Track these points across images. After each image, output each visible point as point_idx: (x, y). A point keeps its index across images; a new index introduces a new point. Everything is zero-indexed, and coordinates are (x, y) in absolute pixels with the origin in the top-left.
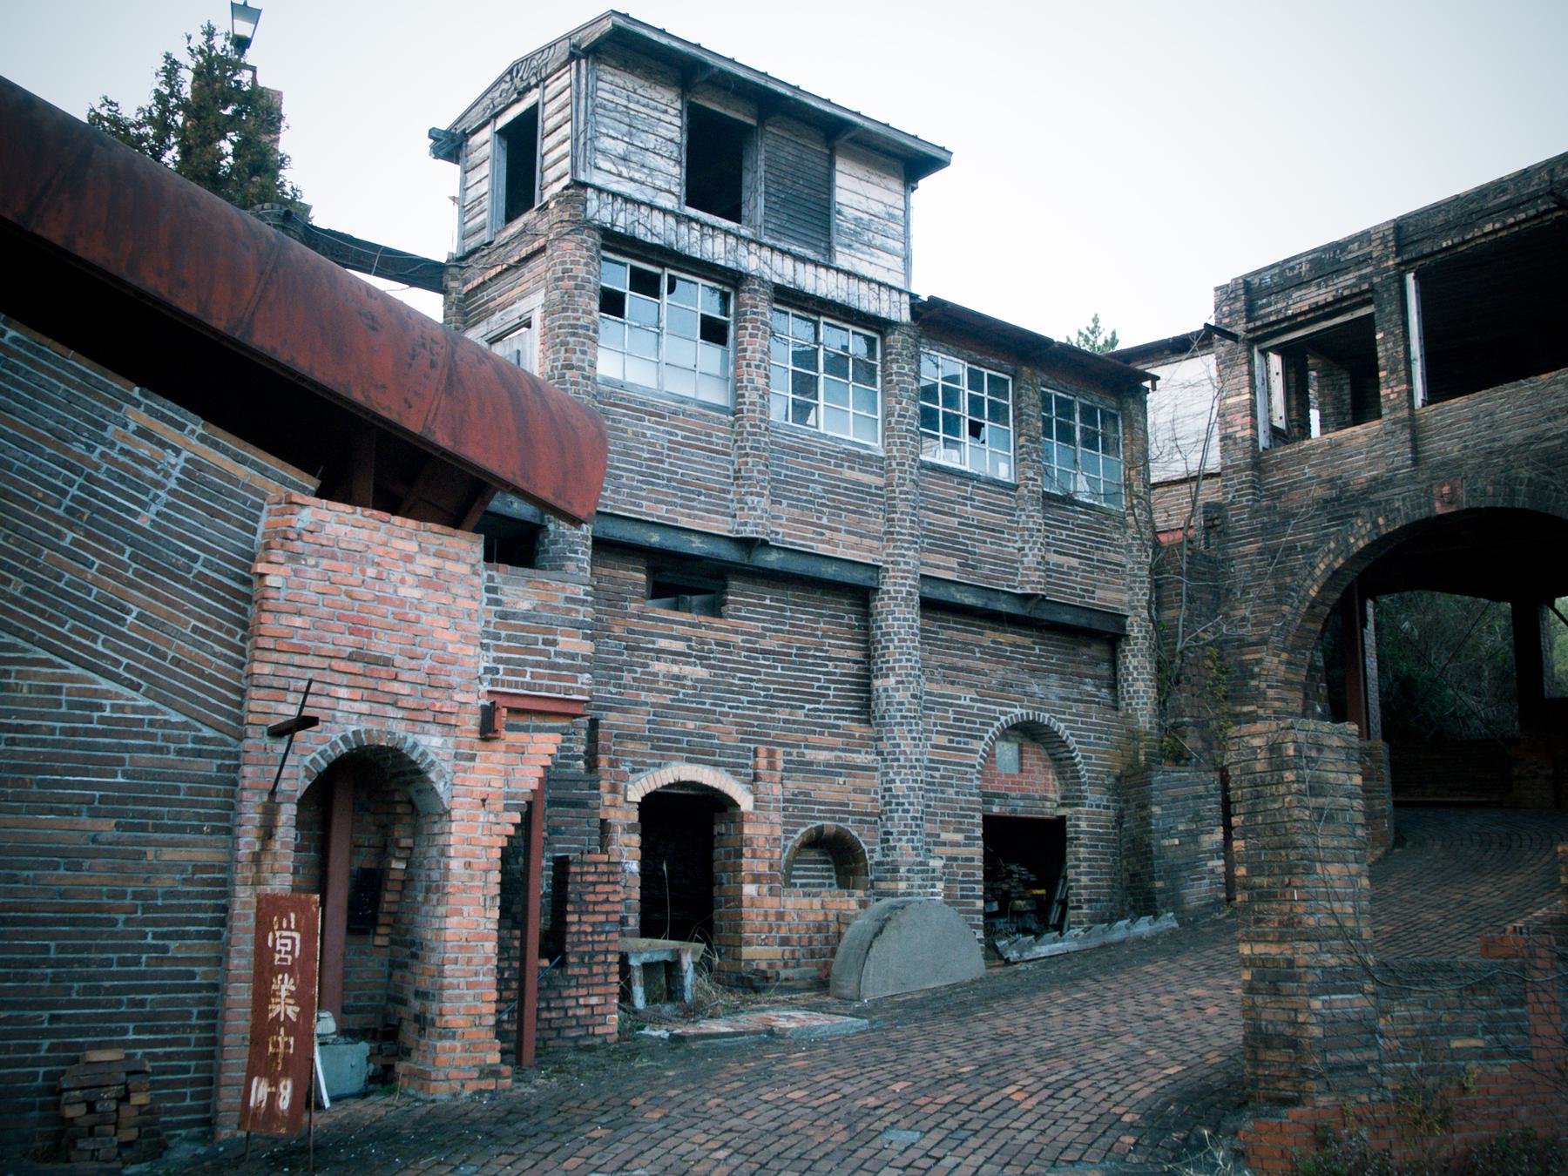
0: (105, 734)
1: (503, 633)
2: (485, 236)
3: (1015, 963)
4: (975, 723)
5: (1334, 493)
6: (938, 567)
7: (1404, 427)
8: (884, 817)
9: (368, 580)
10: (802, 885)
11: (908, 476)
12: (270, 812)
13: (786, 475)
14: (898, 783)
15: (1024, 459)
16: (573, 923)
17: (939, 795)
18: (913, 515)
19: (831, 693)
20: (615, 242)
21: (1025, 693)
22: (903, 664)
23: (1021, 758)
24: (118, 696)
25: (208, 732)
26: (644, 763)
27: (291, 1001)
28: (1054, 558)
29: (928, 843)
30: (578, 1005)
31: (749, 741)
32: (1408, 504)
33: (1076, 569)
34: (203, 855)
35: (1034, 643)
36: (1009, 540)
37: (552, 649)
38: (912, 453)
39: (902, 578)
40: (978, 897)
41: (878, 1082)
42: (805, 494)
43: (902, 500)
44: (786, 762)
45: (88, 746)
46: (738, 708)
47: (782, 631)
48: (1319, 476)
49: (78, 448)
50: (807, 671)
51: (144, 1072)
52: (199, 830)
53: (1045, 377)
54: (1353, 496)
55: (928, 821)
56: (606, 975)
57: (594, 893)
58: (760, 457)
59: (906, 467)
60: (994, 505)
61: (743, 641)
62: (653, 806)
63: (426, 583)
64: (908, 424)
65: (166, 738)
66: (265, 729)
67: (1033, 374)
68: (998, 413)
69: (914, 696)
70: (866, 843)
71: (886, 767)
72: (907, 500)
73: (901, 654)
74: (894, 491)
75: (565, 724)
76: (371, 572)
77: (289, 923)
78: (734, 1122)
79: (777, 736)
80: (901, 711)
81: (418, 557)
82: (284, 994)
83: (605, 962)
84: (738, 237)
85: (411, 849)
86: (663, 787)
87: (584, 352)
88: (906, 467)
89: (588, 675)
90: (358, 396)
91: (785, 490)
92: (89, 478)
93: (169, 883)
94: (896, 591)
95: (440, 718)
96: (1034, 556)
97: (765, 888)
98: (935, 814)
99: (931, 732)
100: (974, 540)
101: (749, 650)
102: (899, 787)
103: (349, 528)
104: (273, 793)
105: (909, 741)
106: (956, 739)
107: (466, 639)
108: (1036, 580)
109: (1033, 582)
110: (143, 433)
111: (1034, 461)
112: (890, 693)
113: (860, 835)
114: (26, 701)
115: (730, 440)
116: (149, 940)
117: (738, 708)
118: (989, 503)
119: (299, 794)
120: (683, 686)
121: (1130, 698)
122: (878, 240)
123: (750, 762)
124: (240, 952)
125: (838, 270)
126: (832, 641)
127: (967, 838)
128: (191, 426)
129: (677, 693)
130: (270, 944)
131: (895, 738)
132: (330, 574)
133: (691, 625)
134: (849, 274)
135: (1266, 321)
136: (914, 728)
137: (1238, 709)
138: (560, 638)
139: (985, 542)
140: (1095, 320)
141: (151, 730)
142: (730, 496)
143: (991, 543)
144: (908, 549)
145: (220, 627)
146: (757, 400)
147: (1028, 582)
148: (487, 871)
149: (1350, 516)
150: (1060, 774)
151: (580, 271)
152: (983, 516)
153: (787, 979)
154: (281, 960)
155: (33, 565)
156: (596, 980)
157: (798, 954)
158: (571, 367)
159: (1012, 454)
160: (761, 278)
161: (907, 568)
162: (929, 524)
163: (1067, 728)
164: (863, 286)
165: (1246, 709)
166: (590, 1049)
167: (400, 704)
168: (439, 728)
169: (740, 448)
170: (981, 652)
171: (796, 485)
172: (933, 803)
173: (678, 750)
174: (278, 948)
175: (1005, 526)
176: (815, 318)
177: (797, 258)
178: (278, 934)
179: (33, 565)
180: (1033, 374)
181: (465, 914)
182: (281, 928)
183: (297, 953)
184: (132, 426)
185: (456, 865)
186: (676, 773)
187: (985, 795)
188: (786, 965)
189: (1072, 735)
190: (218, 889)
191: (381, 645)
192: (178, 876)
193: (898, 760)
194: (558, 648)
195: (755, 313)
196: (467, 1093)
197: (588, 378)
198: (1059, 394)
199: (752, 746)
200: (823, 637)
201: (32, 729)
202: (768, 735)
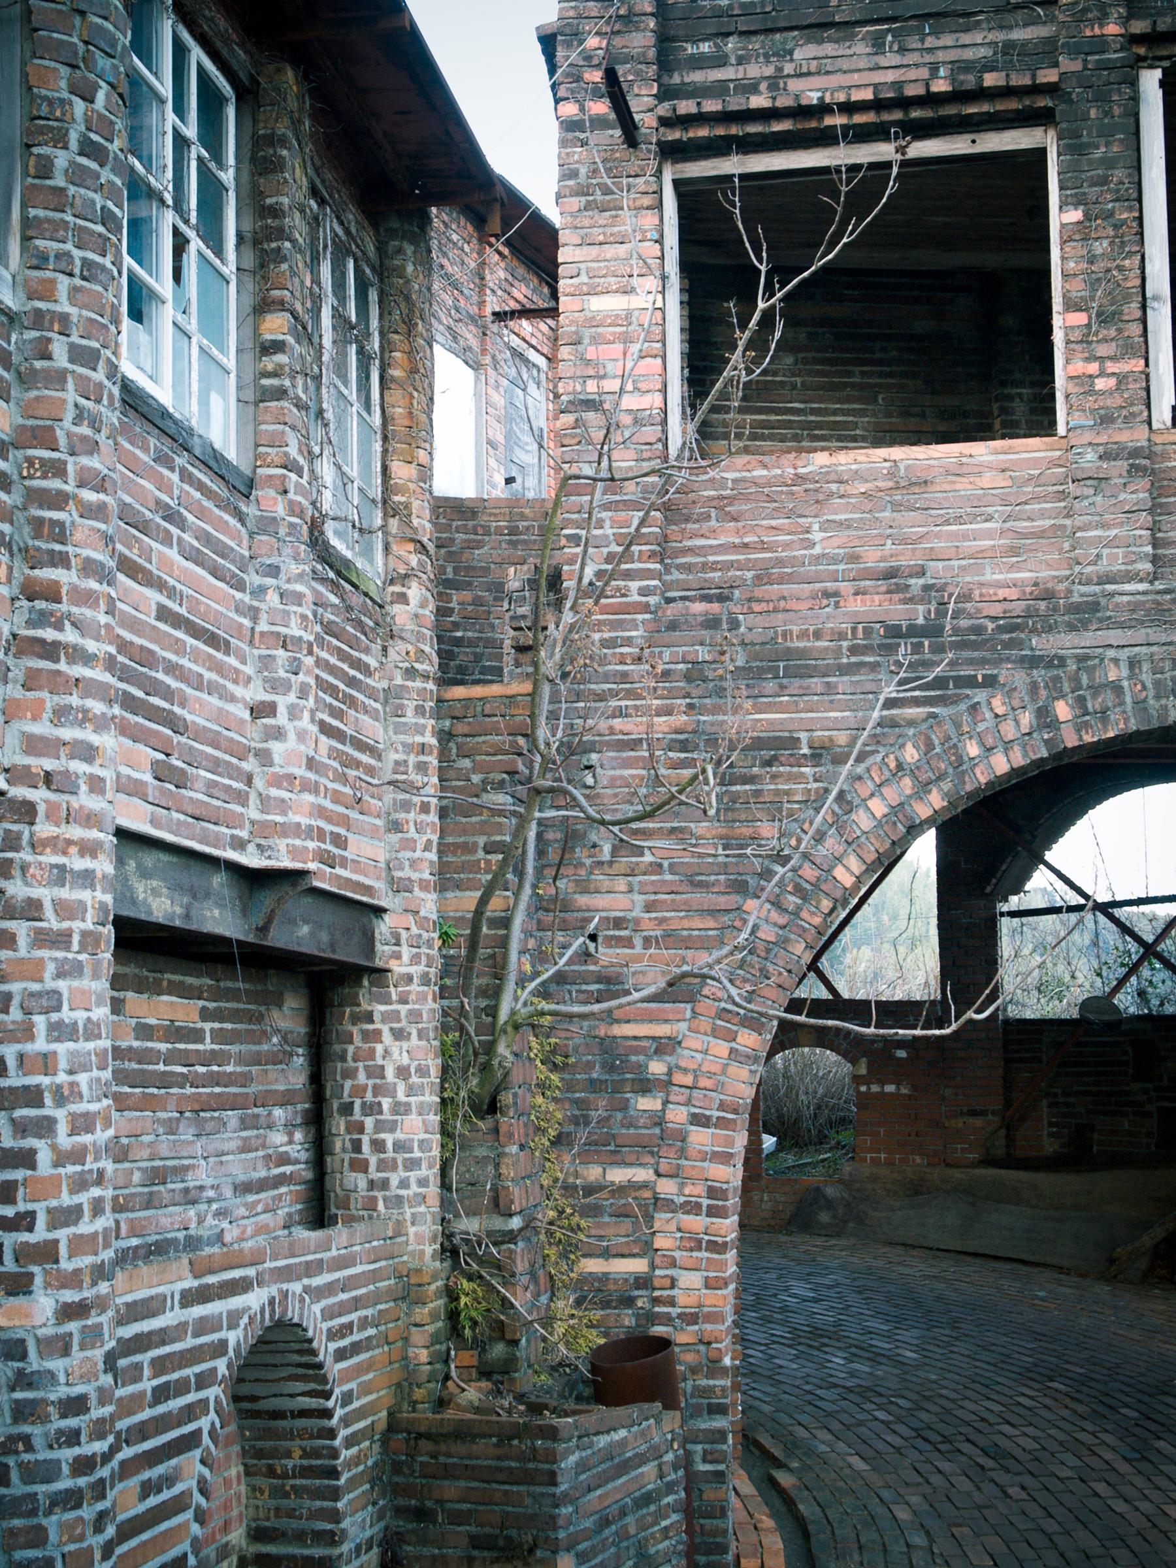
5: (920, 614)
7: (1135, 471)
32: (1147, 677)
35: (205, 1015)
48: (854, 558)
54: (978, 630)
74: (59, 470)
109: (296, 830)
112: (34, 1362)
121: (382, 1166)
135: (736, 104)
137: (593, 1173)
144: (101, 724)
147: (285, 830)
149: (971, 682)
165: (618, 1175)
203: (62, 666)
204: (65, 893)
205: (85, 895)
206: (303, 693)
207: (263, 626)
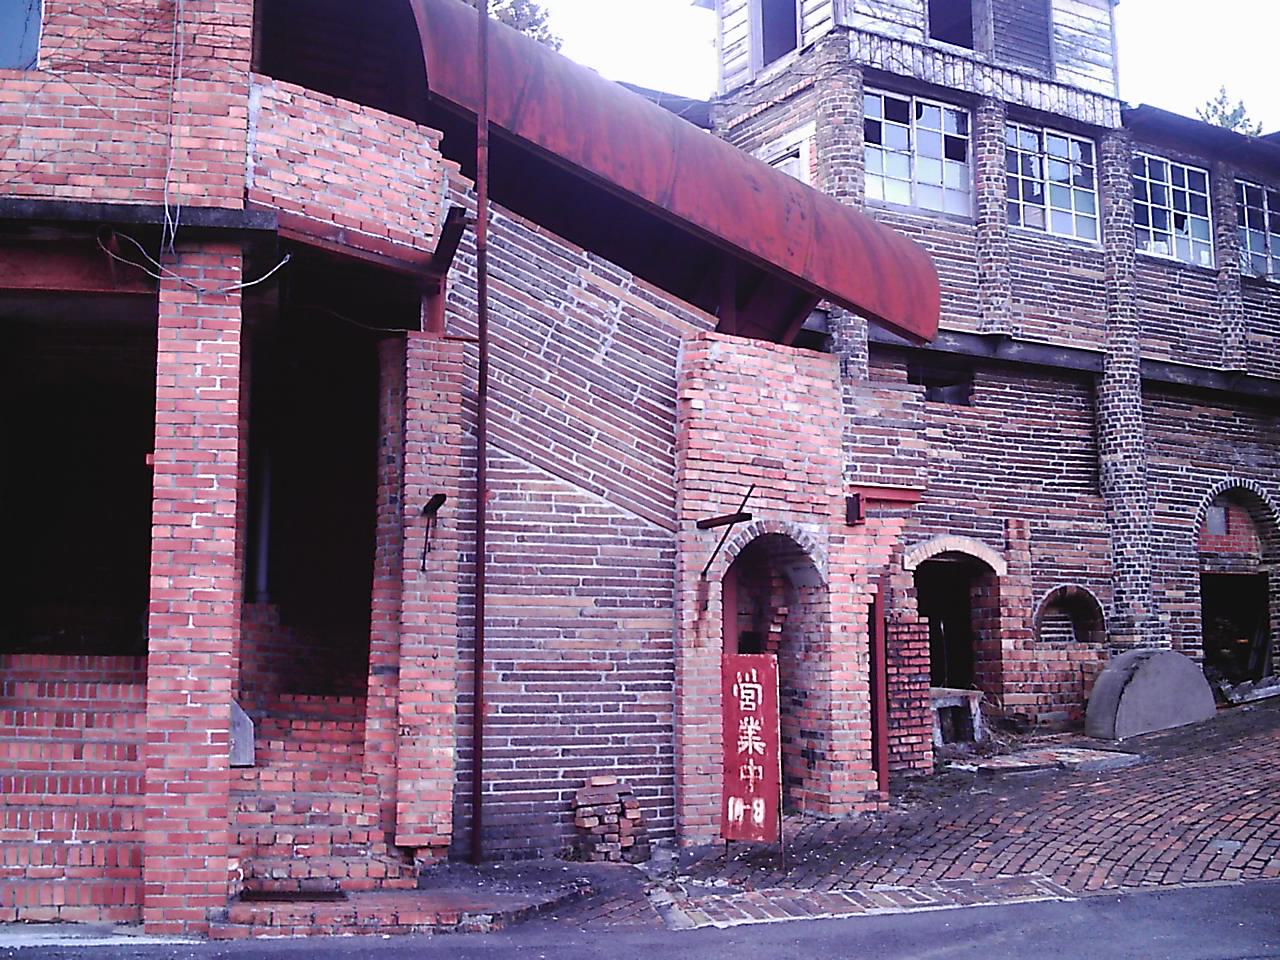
0: (583, 531)
1: (858, 437)
2: (746, 76)
3: (1239, 704)
4: (1191, 491)
6: (1154, 350)
8: (1116, 578)
9: (762, 399)
10: (1047, 640)
11: (1127, 269)
12: (703, 588)
13: (1022, 276)
14: (1129, 548)
15: (1224, 247)
16: (893, 675)
17: (1163, 557)
18: (1133, 305)
19: (1064, 468)
20: (874, 77)
21: (1228, 462)
22: (1130, 440)
23: (1228, 521)
24: (589, 500)
25: (652, 527)
26: (916, 536)
27: (758, 738)
28: (1252, 336)
29: (1155, 601)
30: (901, 744)
31: (1001, 514)
33: (1272, 346)
34: (657, 624)
35: (1235, 415)
36: (1213, 323)
37: (895, 447)
38: (1129, 248)
39: (1125, 362)
40: (1198, 647)
41: (1182, 804)
42: (1040, 291)
43: (1122, 291)
44: (1032, 532)
45: (572, 541)
46: (987, 485)
47: (1021, 415)
49: (549, 305)
50: (1043, 450)
51: (630, 794)
52: (651, 604)
53: (1238, 169)
55: (1155, 581)
56: (922, 718)
57: (908, 649)
58: (1002, 261)
59: (1125, 261)
60: (1200, 290)
61: (989, 426)
62: (926, 573)
63: (801, 398)
64: (1125, 222)
65: (624, 532)
66: (695, 523)
67: (1227, 168)
68: (1198, 206)
69: (1140, 469)
70: (1102, 601)
71: (1117, 533)
72: (1126, 291)
73: (1127, 431)
74: (1115, 284)
75: (907, 510)
76: (764, 392)
77: (751, 677)
78: (1084, 837)
79: (1023, 509)
80: (1129, 482)
81: (795, 377)
82: (750, 733)
83: (920, 707)
84: (974, 63)
85: (786, 615)
86: (933, 556)
87: (854, 180)
88: (1125, 261)
89: (923, 468)
90: (754, 249)
91: (1022, 289)
92: (558, 328)
93: (633, 647)
94: (1120, 375)
95: (818, 509)
96: (1236, 335)
97: (1020, 643)
98: (1161, 574)
99: (1155, 500)
100: (1183, 324)
101: (994, 433)
102: (1129, 551)
103: (747, 357)
104: (704, 574)
105: (1138, 510)
106: (1176, 506)
107: (832, 444)
108: (1239, 357)
109: (1236, 360)
110: (592, 289)
111: (1232, 248)
113: (1097, 594)
114: (529, 507)
115: (974, 247)
116: (623, 692)
117: (987, 485)
118: (1195, 289)
119: (722, 575)
120: (942, 468)
122: (1091, 54)
123: (1002, 533)
124: (689, 700)
125: (1059, 85)
126: (1063, 422)
127: (1187, 595)
128: (624, 281)
129: (937, 474)
130: (736, 693)
131: (1124, 508)
132: (735, 395)
133: (946, 414)
134: (1067, 87)
136: (1141, 497)
138: (900, 438)
139: (1193, 325)
140: (1222, 91)
141: (614, 526)
142: (977, 298)
143: (1198, 326)
145: (655, 442)
146: (997, 210)
147: (1232, 360)
148: (858, 633)
150: (1262, 535)
151: (848, 107)
152: (1190, 301)
153: (1044, 722)
154: (746, 706)
155: (526, 400)
156: (914, 722)
157: (1049, 700)
158: (844, 194)
159: (1211, 242)
160: (996, 98)
161: (1129, 353)
162: (1145, 311)
163: (1269, 492)
164: (1080, 97)
166: (917, 779)
167: (788, 499)
168: (816, 517)
169: (983, 254)
170: (1189, 426)
171: (1030, 284)
172: (1158, 564)
173: (943, 524)
174: (743, 697)
175: (1209, 310)
176: (1039, 130)
177: (1023, 77)
178: (742, 686)
179: (526, 400)
180: (1227, 168)
181: (845, 669)
182: (744, 681)
183: (760, 702)
184: (584, 285)
185: (835, 628)
186: (943, 544)
187: (1200, 555)
188: (1040, 710)
189: (1273, 498)
190: (667, 651)
191: (775, 452)
192: (639, 641)
193: (1128, 527)
194: (899, 447)
195: (992, 131)
196: (856, 814)
197: (859, 202)
198: (1249, 184)
199: (1003, 518)
200: (1055, 418)
201: (535, 528)
202: (1016, 508)
203: (1118, 325)
204: (1121, 372)
205: (1126, 372)
206: (1237, 324)
207: (1223, 308)
